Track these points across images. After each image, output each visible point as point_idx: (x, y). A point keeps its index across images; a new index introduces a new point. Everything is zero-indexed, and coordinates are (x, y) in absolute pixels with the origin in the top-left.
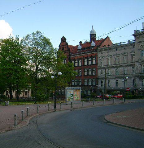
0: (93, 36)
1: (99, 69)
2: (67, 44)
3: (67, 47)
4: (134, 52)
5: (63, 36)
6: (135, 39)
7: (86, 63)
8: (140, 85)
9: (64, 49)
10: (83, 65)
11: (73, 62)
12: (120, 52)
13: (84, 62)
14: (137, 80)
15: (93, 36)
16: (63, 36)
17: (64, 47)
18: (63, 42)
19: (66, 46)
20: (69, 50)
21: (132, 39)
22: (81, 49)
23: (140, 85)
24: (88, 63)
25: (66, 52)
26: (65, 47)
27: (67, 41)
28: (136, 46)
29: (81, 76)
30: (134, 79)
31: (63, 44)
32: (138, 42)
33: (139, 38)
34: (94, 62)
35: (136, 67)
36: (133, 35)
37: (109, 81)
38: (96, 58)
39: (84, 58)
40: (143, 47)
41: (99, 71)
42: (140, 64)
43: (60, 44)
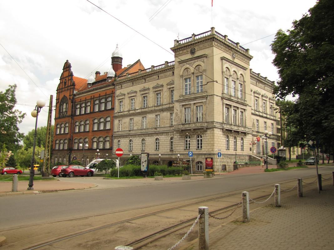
0: (116, 61)
1: (116, 117)
2: (71, 75)
3: (72, 79)
4: (173, 84)
5: (67, 61)
6: (175, 57)
7: (97, 109)
8: (182, 148)
9: (67, 83)
10: (93, 112)
11: (78, 106)
12: (150, 84)
13: (94, 105)
14: (176, 137)
15: (116, 61)
16: (67, 61)
17: (67, 79)
18: (66, 71)
19: (70, 78)
20: (74, 85)
21: (171, 57)
22: (93, 84)
23: (182, 148)
24: (99, 108)
25: (69, 88)
26: (69, 80)
27: (72, 69)
28: (179, 71)
29: (89, 132)
30: (172, 136)
31: (66, 74)
32: (181, 62)
33: (181, 55)
34: (109, 107)
35: (175, 111)
36: (171, 49)
37: (119, 141)
38: (112, 97)
39: (95, 99)
40: (187, 71)
41: (116, 122)
42: (183, 105)
43: (62, 74)
